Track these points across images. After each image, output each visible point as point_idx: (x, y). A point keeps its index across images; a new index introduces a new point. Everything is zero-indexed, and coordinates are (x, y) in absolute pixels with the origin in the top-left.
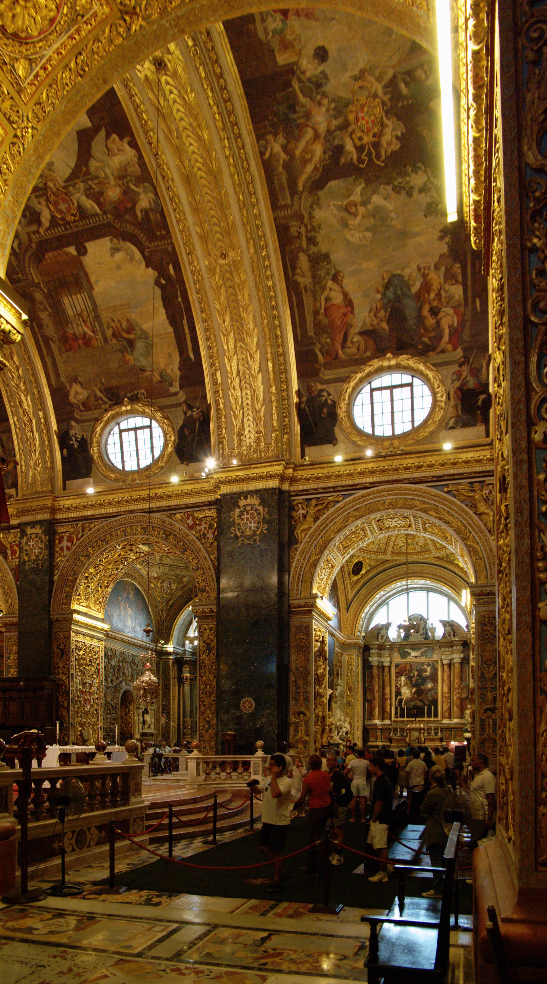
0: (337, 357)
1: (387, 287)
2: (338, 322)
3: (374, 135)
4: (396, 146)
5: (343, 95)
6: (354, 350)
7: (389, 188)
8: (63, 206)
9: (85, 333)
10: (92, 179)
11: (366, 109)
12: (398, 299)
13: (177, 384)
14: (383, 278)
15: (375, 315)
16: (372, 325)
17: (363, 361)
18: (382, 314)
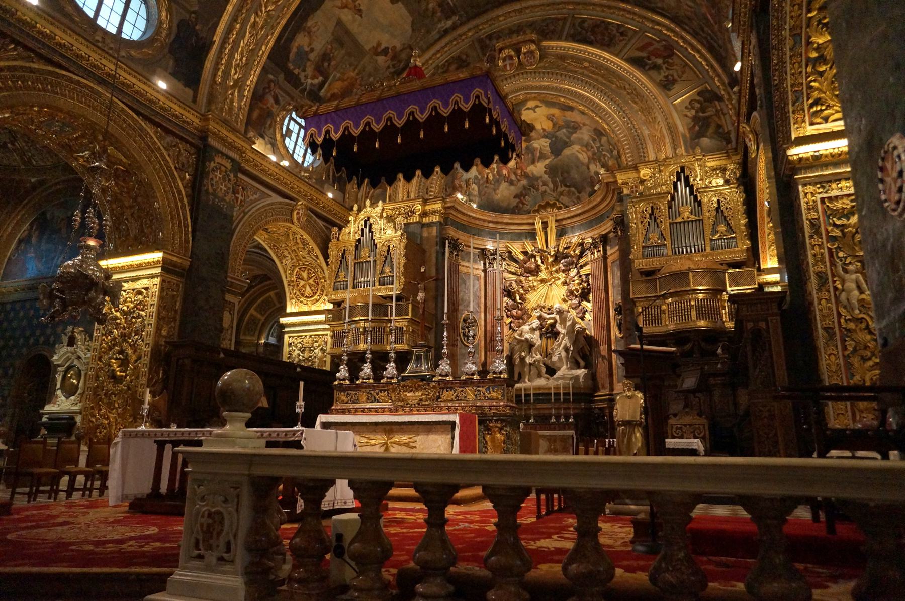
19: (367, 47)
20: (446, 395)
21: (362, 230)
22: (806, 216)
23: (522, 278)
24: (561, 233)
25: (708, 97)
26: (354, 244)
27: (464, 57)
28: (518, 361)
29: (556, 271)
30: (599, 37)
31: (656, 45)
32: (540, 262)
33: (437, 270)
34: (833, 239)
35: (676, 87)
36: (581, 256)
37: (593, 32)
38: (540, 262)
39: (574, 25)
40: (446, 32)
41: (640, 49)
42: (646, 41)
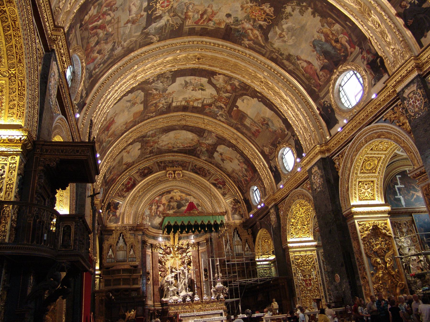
0: (320, 85)
1: (314, 47)
2: (312, 72)
3: (264, 13)
4: (272, 9)
5: (245, 15)
6: (323, 78)
7: (284, 20)
8: (223, 100)
9: (256, 129)
10: (221, 89)
11: (254, 12)
12: (321, 48)
13: (286, 130)
14: (311, 46)
15: (320, 60)
16: (322, 64)
17: (329, 80)
18: (321, 57)
19: (124, 163)
20: (207, 305)
21: (119, 238)
22: (291, 259)
23: (165, 256)
24: (179, 239)
25: (236, 202)
26: (116, 243)
27: (151, 168)
28: (166, 290)
29: (177, 254)
30: (202, 173)
31: (220, 180)
32: (172, 250)
33: (142, 254)
34: (296, 265)
35: (227, 196)
36: (187, 249)
37: (199, 171)
38: (172, 250)
39: (193, 166)
40: (146, 158)
41: (215, 180)
42: (217, 178)
